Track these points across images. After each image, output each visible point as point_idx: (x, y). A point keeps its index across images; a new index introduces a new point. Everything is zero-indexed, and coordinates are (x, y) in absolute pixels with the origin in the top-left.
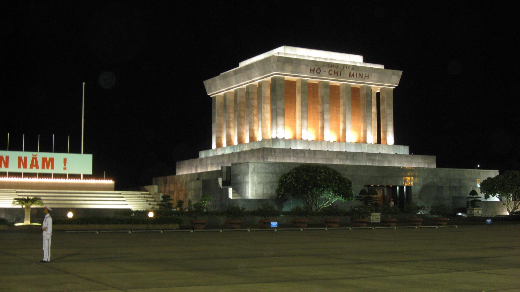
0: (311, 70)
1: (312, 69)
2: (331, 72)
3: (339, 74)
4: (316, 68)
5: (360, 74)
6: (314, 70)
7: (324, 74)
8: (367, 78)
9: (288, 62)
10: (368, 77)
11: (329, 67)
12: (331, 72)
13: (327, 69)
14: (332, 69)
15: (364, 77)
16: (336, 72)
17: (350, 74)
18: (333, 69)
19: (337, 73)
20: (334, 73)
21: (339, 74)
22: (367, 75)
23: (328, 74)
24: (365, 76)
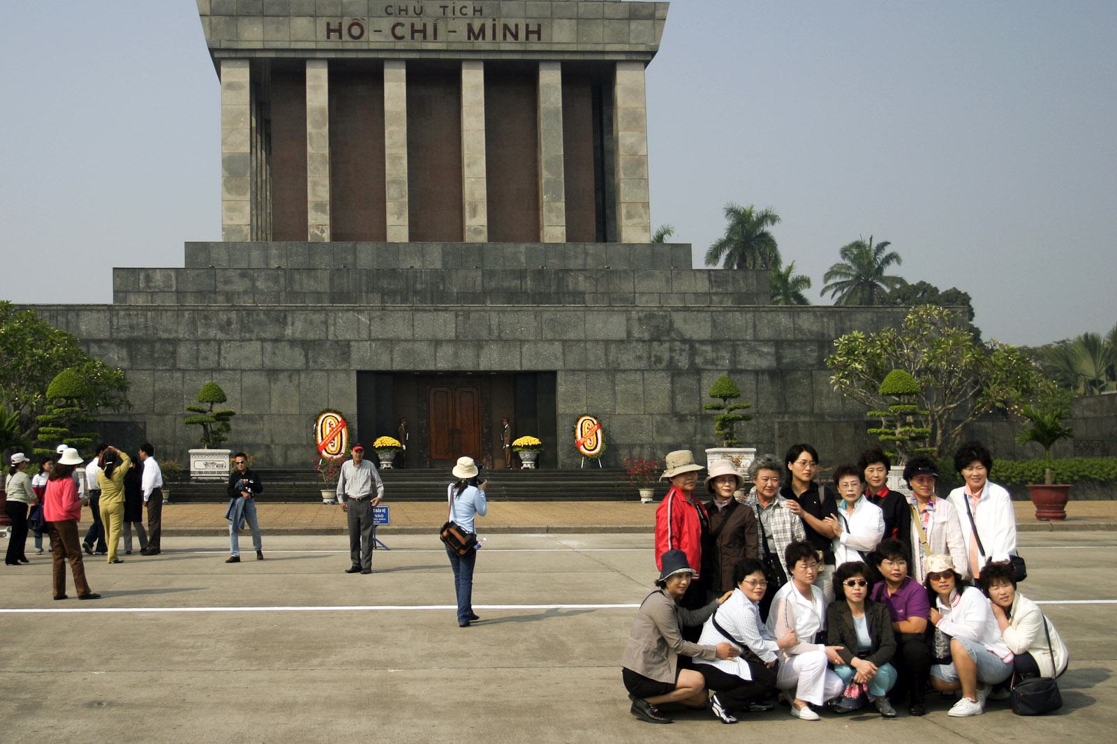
0: (329, 31)
1: (334, 26)
2: (399, 31)
4: (346, 22)
5: (506, 27)
6: (339, 31)
8: (534, 37)
9: (248, 15)
10: (538, 32)
11: (390, 14)
12: (399, 31)
13: (386, 24)
14: (401, 20)
15: (522, 35)
16: (419, 27)
17: (470, 29)
18: (407, 21)
19: (424, 31)
20: (413, 32)
22: (533, 27)
23: (393, 39)
24: (528, 32)
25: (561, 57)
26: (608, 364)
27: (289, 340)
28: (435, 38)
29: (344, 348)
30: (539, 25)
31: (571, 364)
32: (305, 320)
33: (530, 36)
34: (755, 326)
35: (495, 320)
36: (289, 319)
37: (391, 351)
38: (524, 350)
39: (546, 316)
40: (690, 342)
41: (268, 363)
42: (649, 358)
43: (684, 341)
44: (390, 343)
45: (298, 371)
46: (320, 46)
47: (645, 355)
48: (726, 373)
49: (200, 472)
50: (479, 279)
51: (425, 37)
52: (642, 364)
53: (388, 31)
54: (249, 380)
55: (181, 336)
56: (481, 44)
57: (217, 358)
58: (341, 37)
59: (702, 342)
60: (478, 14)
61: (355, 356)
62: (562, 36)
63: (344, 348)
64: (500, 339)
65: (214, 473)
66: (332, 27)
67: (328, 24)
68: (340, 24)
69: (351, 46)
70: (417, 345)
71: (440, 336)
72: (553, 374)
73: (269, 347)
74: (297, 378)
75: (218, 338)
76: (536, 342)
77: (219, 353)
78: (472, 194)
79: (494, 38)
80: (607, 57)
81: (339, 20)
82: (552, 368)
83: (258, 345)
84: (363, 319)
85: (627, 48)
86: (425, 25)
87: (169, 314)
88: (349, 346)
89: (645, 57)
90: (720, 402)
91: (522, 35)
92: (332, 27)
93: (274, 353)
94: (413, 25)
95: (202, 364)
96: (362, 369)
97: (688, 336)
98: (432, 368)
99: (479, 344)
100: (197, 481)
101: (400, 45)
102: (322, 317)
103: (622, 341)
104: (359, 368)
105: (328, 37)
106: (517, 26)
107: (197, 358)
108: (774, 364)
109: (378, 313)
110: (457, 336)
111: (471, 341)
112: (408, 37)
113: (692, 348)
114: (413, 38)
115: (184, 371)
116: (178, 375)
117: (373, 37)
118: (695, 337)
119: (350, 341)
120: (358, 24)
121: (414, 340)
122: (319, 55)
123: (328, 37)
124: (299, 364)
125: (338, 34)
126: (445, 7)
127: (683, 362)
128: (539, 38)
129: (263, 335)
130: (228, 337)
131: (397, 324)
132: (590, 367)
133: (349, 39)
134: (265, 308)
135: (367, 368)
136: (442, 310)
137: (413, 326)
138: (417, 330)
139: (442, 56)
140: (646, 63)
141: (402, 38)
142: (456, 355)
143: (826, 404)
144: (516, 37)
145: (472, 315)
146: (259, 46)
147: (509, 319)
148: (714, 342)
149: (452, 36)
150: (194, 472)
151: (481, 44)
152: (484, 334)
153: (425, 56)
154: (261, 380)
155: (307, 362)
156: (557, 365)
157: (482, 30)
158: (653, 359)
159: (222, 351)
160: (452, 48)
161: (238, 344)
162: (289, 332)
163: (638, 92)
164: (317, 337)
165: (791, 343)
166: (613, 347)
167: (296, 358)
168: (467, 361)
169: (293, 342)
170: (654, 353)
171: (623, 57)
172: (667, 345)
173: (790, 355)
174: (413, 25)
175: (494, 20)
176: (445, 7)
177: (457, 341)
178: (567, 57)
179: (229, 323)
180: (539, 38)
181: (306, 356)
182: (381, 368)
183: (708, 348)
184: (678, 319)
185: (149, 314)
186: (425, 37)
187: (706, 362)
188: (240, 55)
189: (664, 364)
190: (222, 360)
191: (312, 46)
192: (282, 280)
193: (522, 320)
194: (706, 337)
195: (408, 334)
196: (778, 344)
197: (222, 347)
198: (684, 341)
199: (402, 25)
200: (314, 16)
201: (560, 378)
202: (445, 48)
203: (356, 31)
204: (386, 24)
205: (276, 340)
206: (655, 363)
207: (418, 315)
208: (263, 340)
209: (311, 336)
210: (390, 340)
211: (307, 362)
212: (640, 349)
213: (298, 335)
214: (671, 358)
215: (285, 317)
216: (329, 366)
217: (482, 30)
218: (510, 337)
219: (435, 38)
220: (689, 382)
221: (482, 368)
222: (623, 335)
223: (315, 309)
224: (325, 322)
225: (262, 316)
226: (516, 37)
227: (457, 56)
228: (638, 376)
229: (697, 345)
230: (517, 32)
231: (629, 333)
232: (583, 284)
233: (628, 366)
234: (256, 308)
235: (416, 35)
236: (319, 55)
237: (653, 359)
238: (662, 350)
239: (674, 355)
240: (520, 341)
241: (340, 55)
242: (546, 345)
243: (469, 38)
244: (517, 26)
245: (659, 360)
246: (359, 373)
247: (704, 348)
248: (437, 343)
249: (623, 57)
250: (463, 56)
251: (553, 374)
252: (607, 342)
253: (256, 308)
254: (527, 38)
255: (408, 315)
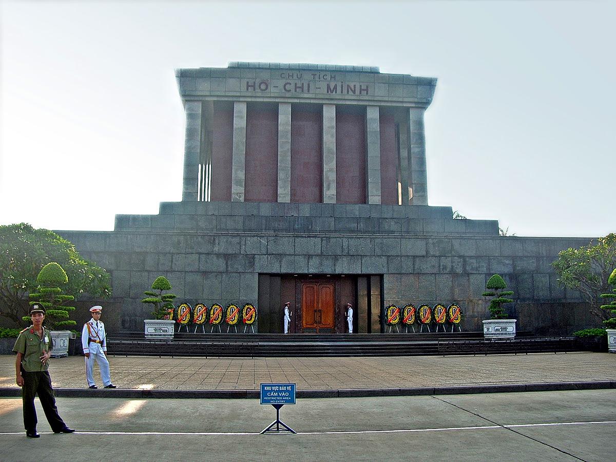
0: (248, 86)
2: (288, 87)
3: (305, 88)
4: (258, 81)
5: (348, 86)
6: (254, 86)
7: (275, 90)
10: (367, 90)
12: (288, 87)
13: (281, 83)
14: (288, 81)
15: (357, 92)
18: (292, 82)
19: (302, 88)
20: (296, 87)
21: (305, 88)
23: (284, 91)
25: (379, 104)
26: (414, 270)
27: (216, 254)
28: (308, 91)
29: (251, 259)
30: (367, 87)
31: (392, 270)
32: (227, 241)
33: (362, 92)
34: (501, 248)
35: (345, 244)
36: (217, 241)
37: (280, 261)
38: (363, 261)
39: (378, 241)
40: (463, 257)
41: (202, 268)
42: (439, 266)
43: (460, 257)
44: (280, 256)
45: (221, 272)
46: (243, 94)
47: (437, 265)
48: (484, 275)
49: (151, 335)
50: (333, 223)
51: (303, 91)
52: (435, 270)
53: (281, 87)
54: (190, 278)
55: (148, 250)
56: (334, 95)
57: (170, 264)
58: (254, 90)
59: (471, 257)
60: (333, 79)
61: (257, 265)
62: (380, 92)
63: (251, 259)
64: (348, 255)
65: (160, 335)
66: (249, 84)
67: (248, 83)
68: (255, 83)
69: (260, 94)
70: (297, 258)
71: (311, 252)
72: (381, 276)
73: (203, 257)
74: (220, 277)
75: (171, 251)
76: (370, 256)
77: (172, 261)
78: (328, 178)
79: (342, 92)
80: (405, 105)
81: (254, 80)
82: (381, 272)
83: (197, 256)
84: (264, 241)
85: (416, 100)
86: (303, 84)
87: (142, 236)
88: (254, 258)
89: (424, 104)
90: (493, 291)
91: (357, 92)
92: (249, 84)
93: (206, 262)
94: (296, 84)
95: (161, 268)
96: (262, 272)
97: (462, 254)
98: (306, 272)
99: (336, 258)
100: (150, 340)
101: (288, 95)
102: (237, 240)
103: (423, 256)
104: (260, 271)
105: (247, 90)
106: (355, 86)
107: (158, 264)
108: (512, 271)
109: (273, 238)
110: (322, 253)
111: (331, 256)
112: (293, 91)
113: (465, 261)
114: (296, 91)
115: (149, 271)
116: (146, 274)
117: (273, 90)
118: (466, 254)
119: (255, 255)
120: (265, 83)
121: (295, 255)
122: (241, 99)
123: (247, 90)
124: (222, 268)
125: (253, 88)
126: (314, 75)
127: (459, 270)
128: (367, 94)
129: (200, 251)
130: (178, 251)
131: (285, 244)
132: (403, 272)
133: (259, 91)
134: (202, 234)
135: (265, 272)
136: (313, 237)
137: (294, 246)
138: (297, 249)
139: (312, 101)
140: (425, 108)
141: (290, 90)
142: (321, 264)
143: (541, 294)
144: (354, 92)
145: (332, 240)
146: (208, 94)
147: (352, 242)
148: (477, 257)
149: (318, 91)
150: (147, 335)
151: (334, 95)
152: (339, 252)
153: (302, 101)
154: (198, 278)
155: (227, 267)
156: (383, 270)
157: (335, 88)
158: (441, 267)
159: (174, 260)
160: (318, 97)
161: (184, 255)
162: (216, 249)
163: (420, 124)
164: (234, 252)
165: (521, 258)
166: (417, 259)
167: (221, 264)
168: (328, 269)
169: (218, 255)
170: (442, 264)
171: (413, 105)
172: (450, 259)
173: (520, 265)
174: (296, 84)
175: (342, 83)
176: (314, 75)
177: (321, 255)
178: (383, 104)
179: (179, 243)
180: (367, 94)
181: (227, 263)
182: (274, 271)
183: (474, 261)
184: (456, 244)
185: (129, 236)
186: (303, 91)
187: (473, 269)
188: (196, 99)
189: (448, 270)
190: (173, 265)
191: (238, 94)
192: (214, 222)
193: (362, 244)
194: (472, 255)
195: (292, 252)
196: (514, 258)
197: (174, 258)
198: (460, 257)
199: (290, 84)
200: (240, 78)
201: (386, 279)
202: (314, 97)
203: (263, 87)
204: (281, 83)
205: (208, 254)
206: (443, 269)
207: (297, 240)
208: (200, 254)
209: (230, 252)
210: (280, 255)
211: (227, 267)
212: (434, 261)
213: (221, 251)
214: (452, 266)
215: (214, 239)
216: (240, 270)
217: (335, 88)
218: (355, 254)
219: (308, 91)
220: (464, 280)
221: (337, 272)
222: (424, 253)
223: (234, 235)
224: (240, 243)
225: (200, 239)
226: (354, 92)
227: (321, 102)
228: (432, 278)
229: (467, 259)
230: (355, 90)
231: (427, 252)
232: (393, 226)
233: (426, 272)
234: (196, 234)
235: (298, 90)
236: (241, 99)
237: (441, 267)
238: (446, 262)
239: (454, 264)
240: (361, 256)
241: (253, 100)
242: (377, 258)
243: (328, 92)
244: (355, 86)
245: (445, 268)
246: (260, 274)
247: (471, 261)
248: (309, 257)
249: (413, 105)
250: (324, 102)
251: (381, 276)
252: (414, 257)
253: (196, 234)
254: (360, 93)
255: (291, 240)
